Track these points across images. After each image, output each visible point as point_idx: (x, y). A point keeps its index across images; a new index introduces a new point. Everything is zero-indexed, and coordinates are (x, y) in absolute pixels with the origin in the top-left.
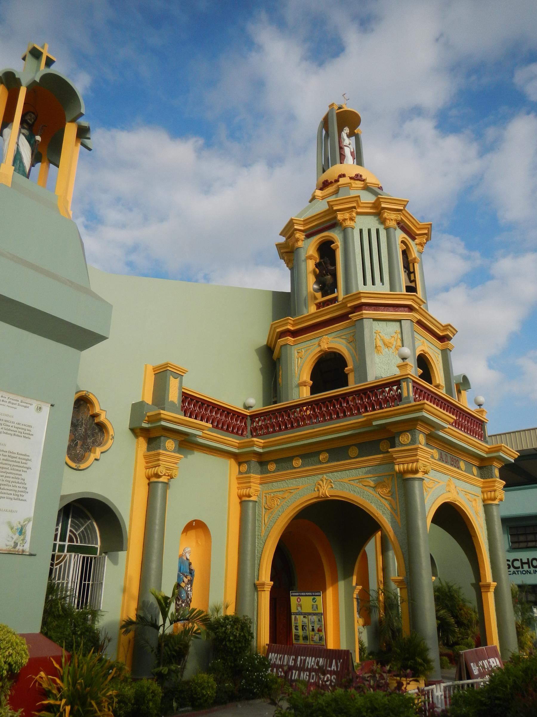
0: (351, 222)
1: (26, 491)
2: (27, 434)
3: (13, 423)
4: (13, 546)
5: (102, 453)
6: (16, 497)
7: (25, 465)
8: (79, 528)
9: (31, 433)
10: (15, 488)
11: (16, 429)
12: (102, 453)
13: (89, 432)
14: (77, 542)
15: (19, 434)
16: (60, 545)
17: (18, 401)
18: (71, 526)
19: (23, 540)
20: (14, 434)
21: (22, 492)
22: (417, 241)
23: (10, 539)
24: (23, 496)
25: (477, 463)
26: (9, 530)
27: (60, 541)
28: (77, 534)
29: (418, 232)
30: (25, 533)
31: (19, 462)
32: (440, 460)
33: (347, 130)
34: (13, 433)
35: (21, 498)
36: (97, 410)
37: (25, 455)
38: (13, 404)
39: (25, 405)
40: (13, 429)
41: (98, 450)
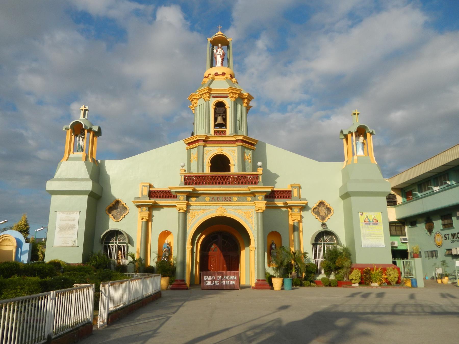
0: (195, 104)
4: (72, 244)
8: (122, 237)
13: (122, 210)
14: (121, 241)
16: (115, 242)
18: (119, 237)
19: (75, 243)
22: (230, 96)
25: (252, 195)
27: (116, 241)
28: (121, 239)
29: (228, 92)
32: (212, 200)
36: (122, 203)
41: (124, 215)
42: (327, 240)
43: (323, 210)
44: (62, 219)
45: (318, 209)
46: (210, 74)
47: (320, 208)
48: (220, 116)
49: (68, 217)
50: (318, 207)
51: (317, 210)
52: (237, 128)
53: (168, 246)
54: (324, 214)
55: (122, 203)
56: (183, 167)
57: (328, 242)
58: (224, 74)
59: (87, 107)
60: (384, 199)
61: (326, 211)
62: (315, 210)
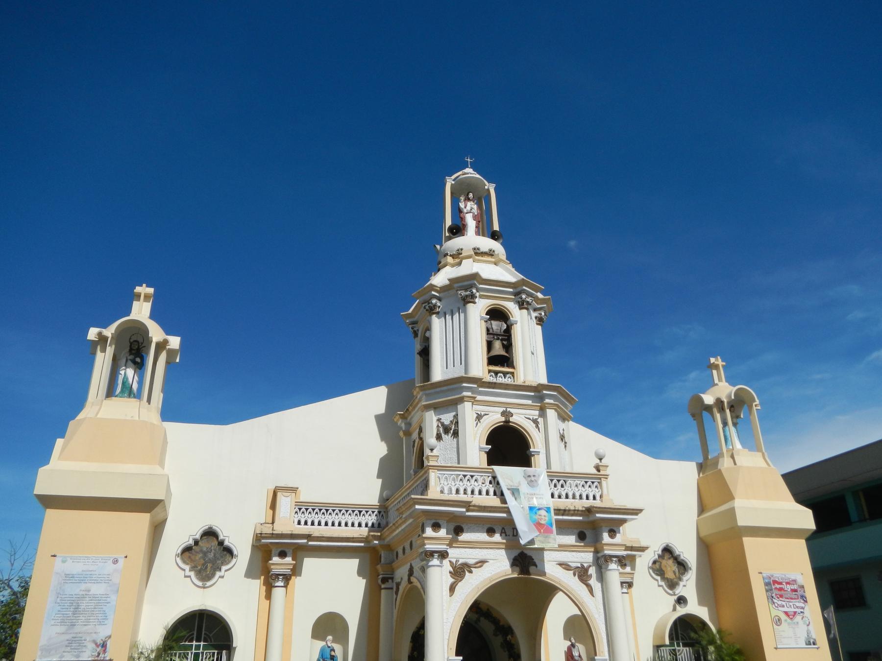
1: (107, 618)
2: (108, 580)
3: (96, 575)
4: (97, 655)
5: (226, 571)
6: (99, 623)
7: (105, 601)
9: (109, 579)
10: (98, 618)
11: (98, 579)
12: (226, 571)
13: (217, 555)
15: (101, 581)
16: (196, 645)
17: (99, 559)
18: (205, 631)
20: (97, 582)
21: (104, 619)
23: (95, 651)
24: (104, 622)
26: (94, 646)
28: (211, 635)
30: (106, 644)
31: (100, 600)
33: (462, 198)
34: (96, 582)
35: (103, 623)
37: (106, 595)
38: (95, 562)
39: (104, 561)
40: (95, 579)
41: (224, 568)
42: (685, 637)
43: (671, 567)
44: (69, 578)
45: (659, 563)
46: (462, 249)
47: (664, 562)
48: (496, 339)
49: (90, 573)
50: (660, 560)
51: (657, 566)
53: (333, 653)
54: (673, 574)
55: (221, 537)
57: (687, 640)
58: (491, 253)
60: (803, 542)
61: (675, 568)
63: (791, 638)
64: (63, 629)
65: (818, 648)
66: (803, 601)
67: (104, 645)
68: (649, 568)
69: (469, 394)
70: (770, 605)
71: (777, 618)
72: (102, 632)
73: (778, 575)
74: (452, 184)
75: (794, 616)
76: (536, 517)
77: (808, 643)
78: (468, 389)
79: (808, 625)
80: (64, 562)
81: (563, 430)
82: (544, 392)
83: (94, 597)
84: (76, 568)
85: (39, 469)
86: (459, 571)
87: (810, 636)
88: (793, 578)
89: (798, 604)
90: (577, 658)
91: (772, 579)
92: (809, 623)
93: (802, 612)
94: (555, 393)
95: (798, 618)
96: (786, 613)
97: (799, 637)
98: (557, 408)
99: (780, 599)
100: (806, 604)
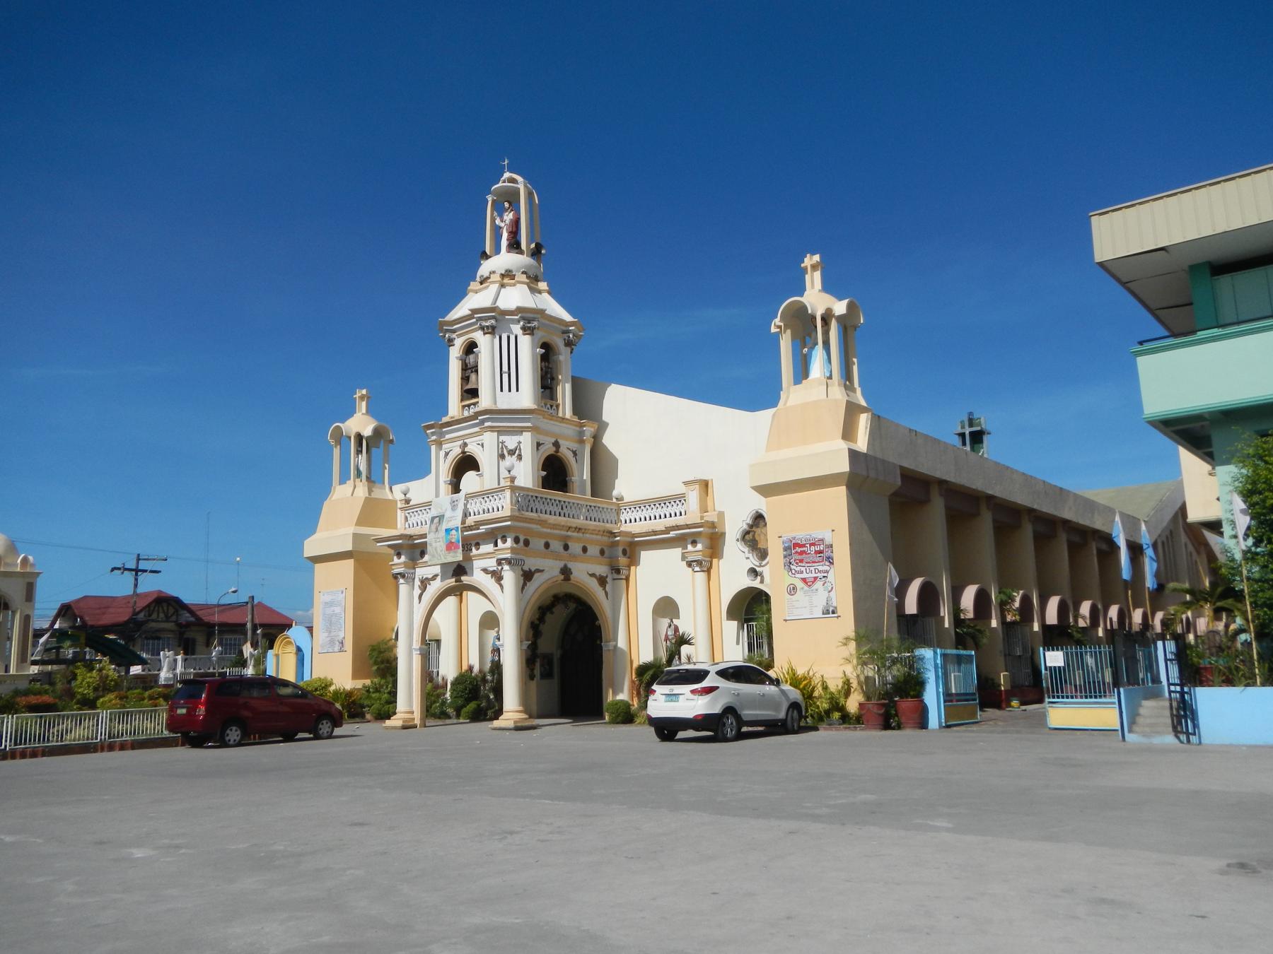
33: (495, 214)
44: (326, 603)
48: (472, 372)
52: (502, 390)
56: (405, 495)
59: (364, 392)
60: (841, 491)
62: (747, 537)
63: (805, 607)
64: (326, 634)
65: (838, 617)
66: (829, 564)
67: (342, 643)
68: (738, 540)
69: (434, 438)
70: (786, 572)
71: (792, 586)
72: (342, 635)
73: (801, 534)
74: (494, 201)
75: (813, 582)
76: (449, 537)
77: (826, 612)
78: (433, 434)
79: (829, 592)
80: (324, 595)
81: (520, 443)
82: (479, 418)
83: (336, 615)
84: (327, 598)
85: (306, 542)
86: (425, 583)
87: (830, 603)
88: (820, 537)
89: (820, 568)
90: (670, 637)
91: (794, 542)
92: (832, 588)
93: (824, 577)
94: (487, 416)
95: (819, 584)
96: (804, 580)
97: (816, 606)
98: (491, 429)
99: (800, 564)
100: (832, 566)
